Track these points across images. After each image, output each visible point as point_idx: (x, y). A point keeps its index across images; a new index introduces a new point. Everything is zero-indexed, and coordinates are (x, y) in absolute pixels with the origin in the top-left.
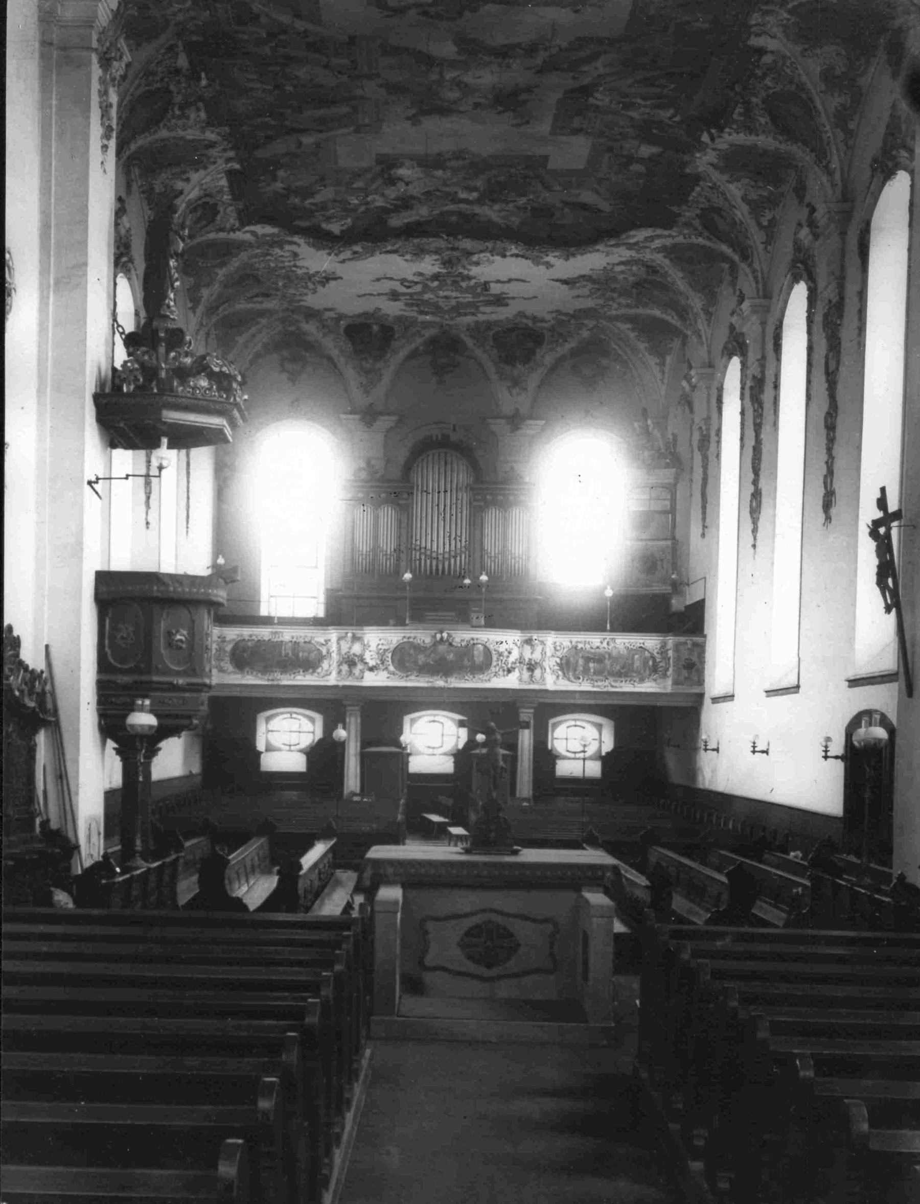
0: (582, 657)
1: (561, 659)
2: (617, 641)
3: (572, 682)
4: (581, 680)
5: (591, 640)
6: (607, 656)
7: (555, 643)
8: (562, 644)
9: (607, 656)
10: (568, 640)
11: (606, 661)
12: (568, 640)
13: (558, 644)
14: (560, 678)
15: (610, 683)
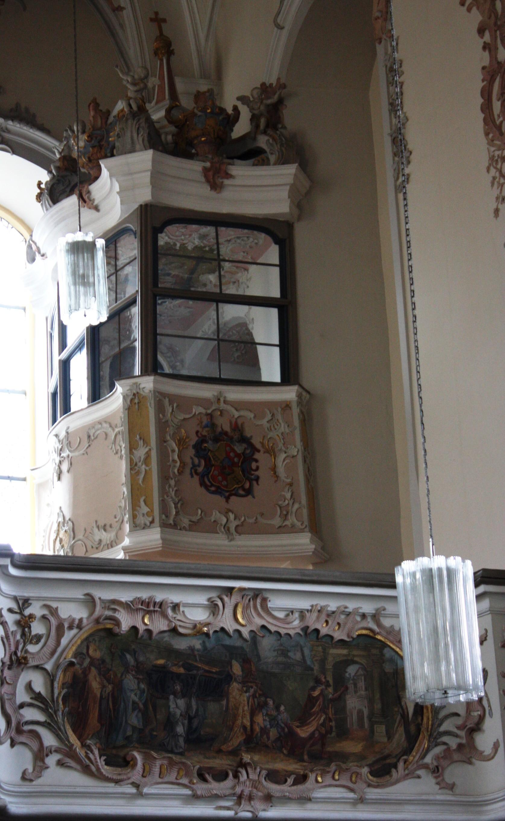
0: (139, 668)
1: (51, 678)
2: (275, 602)
3: (100, 776)
4: (136, 774)
5: (175, 597)
6: (237, 669)
7: (26, 602)
8: (54, 612)
9: (237, 669)
10: (79, 593)
11: (235, 686)
12: (79, 593)
13: (35, 609)
14: (52, 760)
15: (255, 785)
